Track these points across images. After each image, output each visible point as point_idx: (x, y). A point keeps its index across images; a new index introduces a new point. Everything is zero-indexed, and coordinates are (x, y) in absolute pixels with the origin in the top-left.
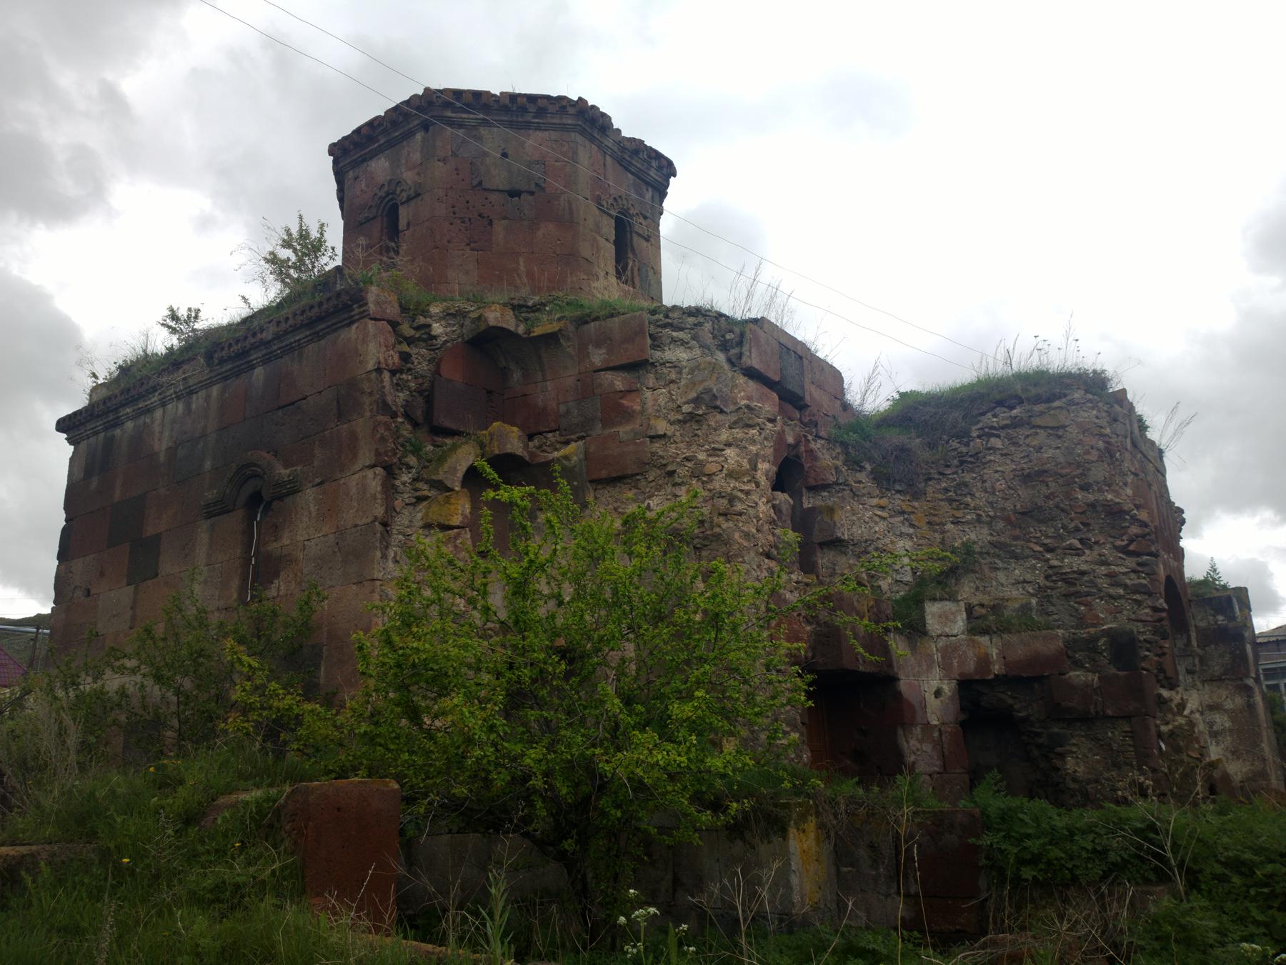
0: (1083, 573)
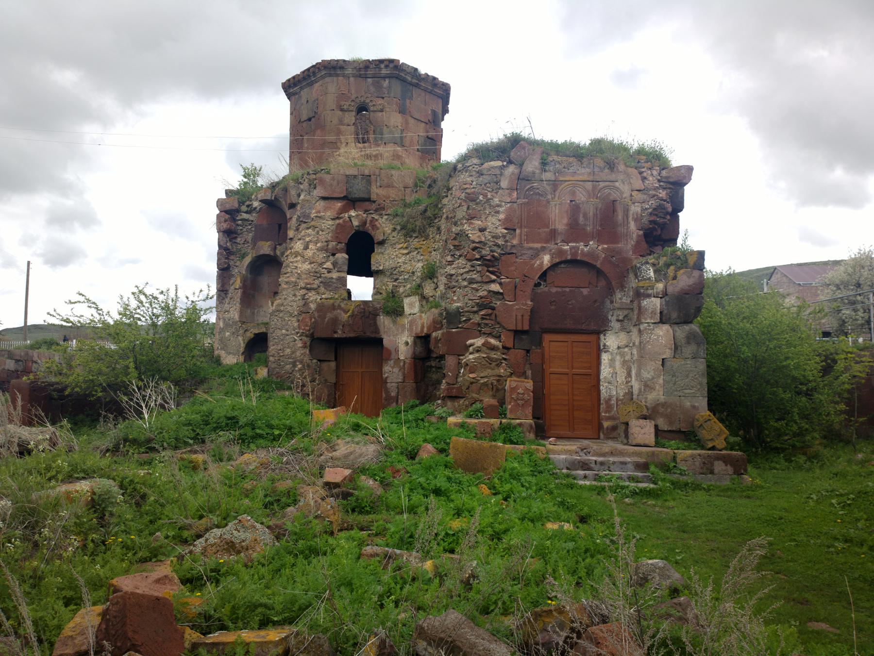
0: (452, 275)
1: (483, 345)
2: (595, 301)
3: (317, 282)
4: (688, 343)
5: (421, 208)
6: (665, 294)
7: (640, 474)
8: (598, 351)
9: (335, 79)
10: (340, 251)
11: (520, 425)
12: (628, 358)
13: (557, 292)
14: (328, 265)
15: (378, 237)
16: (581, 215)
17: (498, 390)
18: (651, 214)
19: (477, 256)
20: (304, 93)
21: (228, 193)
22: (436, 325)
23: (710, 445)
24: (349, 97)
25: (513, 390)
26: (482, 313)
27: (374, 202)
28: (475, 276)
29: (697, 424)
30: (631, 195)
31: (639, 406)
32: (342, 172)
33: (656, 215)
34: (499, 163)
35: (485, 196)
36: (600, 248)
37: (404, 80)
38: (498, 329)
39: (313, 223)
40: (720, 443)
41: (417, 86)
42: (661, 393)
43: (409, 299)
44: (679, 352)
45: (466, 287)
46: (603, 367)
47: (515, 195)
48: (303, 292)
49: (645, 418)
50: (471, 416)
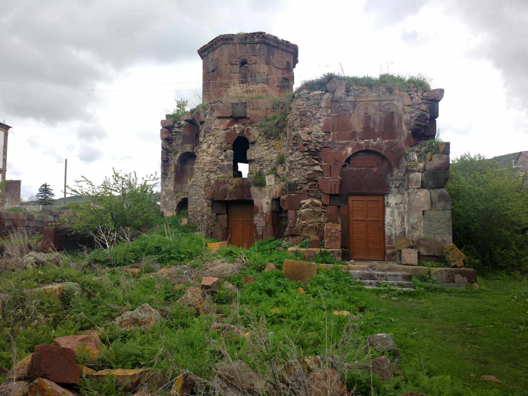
0: (292, 161)
1: (310, 203)
2: (381, 175)
3: (215, 167)
4: (439, 200)
5: (276, 121)
6: (424, 170)
7: (406, 282)
8: (384, 206)
9: (227, 46)
10: (229, 149)
11: (332, 252)
12: (402, 210)
13: (357, 170)
14: (222, 157)
15: (251, 140)
16: (372, 123)
17: (319, 231)
18: (416, 120)
19: (306, 150)
20: (210, 56)
21: (168, 116)
22: (283, 192)
23: (453, 264)
24: (236, 57)
25: (329, 230)
26: (310, 184)
27: (249, 119)
28: (305, 162)
29: (445, 251)
30: (403, 109)
31: (408, 240)
32: (229, 101)
33: (420, 121)
34: (320, 92)
35: (311, 112)
36: (384, 142)
37: (269, 45)
38: (320, 193)
39: (213, 133)
40: (460, 263)
41: (277, 47)
42: (422, 232)
43: (268, 176)
44: (434, 206)
45: (300, 168)
46: (386, 216)
47: (330, 111)
48: (207, 173)
49: (412, 247)
50: (302, 247)
